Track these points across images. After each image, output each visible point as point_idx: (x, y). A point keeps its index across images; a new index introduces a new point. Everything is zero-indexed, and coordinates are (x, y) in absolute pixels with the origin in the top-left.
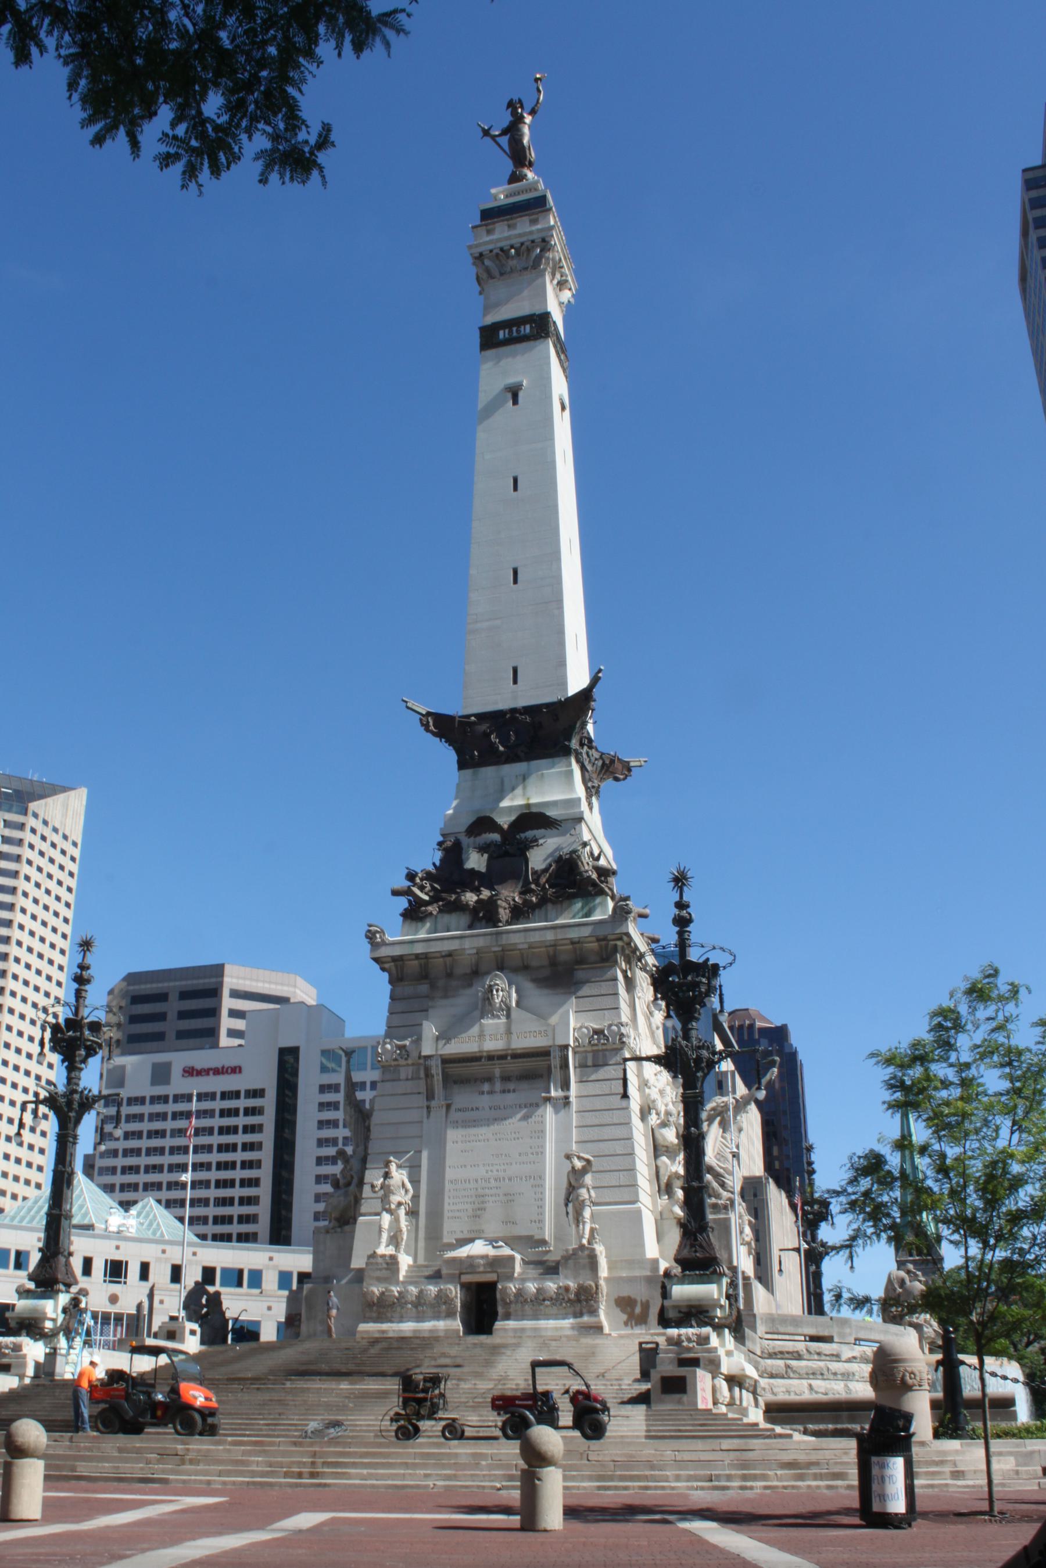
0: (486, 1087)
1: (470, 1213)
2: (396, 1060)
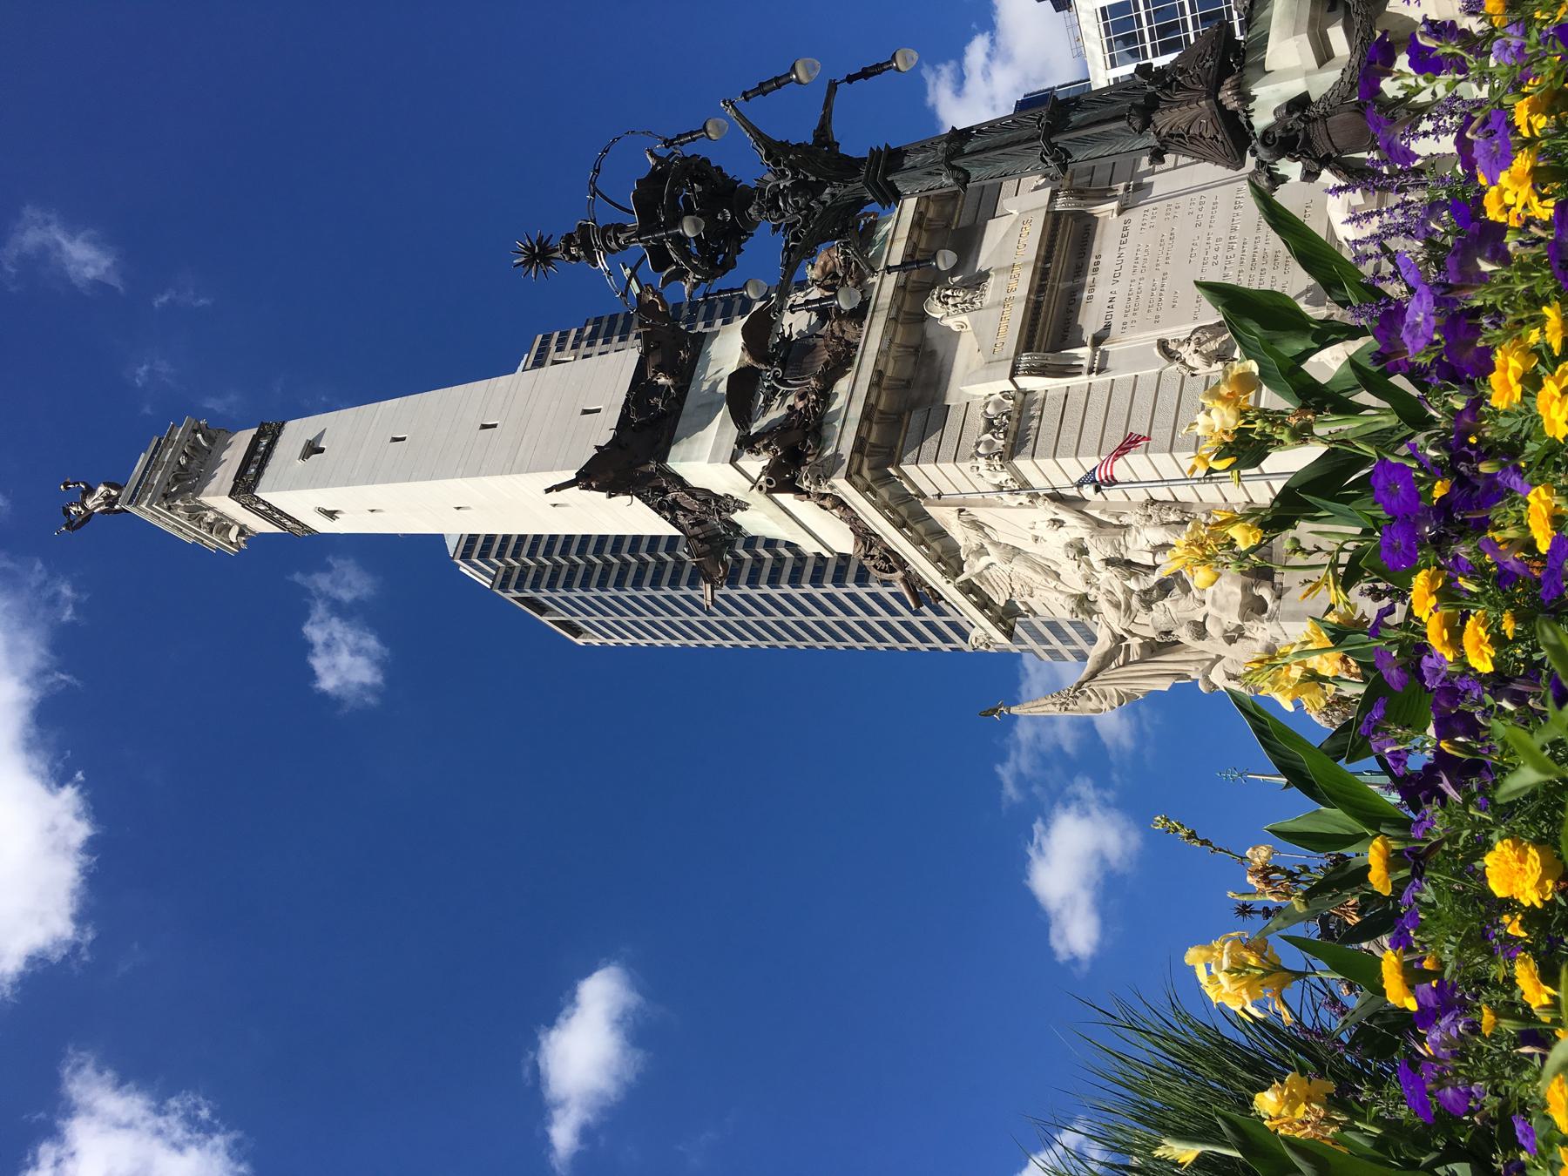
0: (1086, 294)
2: (1005, 433)
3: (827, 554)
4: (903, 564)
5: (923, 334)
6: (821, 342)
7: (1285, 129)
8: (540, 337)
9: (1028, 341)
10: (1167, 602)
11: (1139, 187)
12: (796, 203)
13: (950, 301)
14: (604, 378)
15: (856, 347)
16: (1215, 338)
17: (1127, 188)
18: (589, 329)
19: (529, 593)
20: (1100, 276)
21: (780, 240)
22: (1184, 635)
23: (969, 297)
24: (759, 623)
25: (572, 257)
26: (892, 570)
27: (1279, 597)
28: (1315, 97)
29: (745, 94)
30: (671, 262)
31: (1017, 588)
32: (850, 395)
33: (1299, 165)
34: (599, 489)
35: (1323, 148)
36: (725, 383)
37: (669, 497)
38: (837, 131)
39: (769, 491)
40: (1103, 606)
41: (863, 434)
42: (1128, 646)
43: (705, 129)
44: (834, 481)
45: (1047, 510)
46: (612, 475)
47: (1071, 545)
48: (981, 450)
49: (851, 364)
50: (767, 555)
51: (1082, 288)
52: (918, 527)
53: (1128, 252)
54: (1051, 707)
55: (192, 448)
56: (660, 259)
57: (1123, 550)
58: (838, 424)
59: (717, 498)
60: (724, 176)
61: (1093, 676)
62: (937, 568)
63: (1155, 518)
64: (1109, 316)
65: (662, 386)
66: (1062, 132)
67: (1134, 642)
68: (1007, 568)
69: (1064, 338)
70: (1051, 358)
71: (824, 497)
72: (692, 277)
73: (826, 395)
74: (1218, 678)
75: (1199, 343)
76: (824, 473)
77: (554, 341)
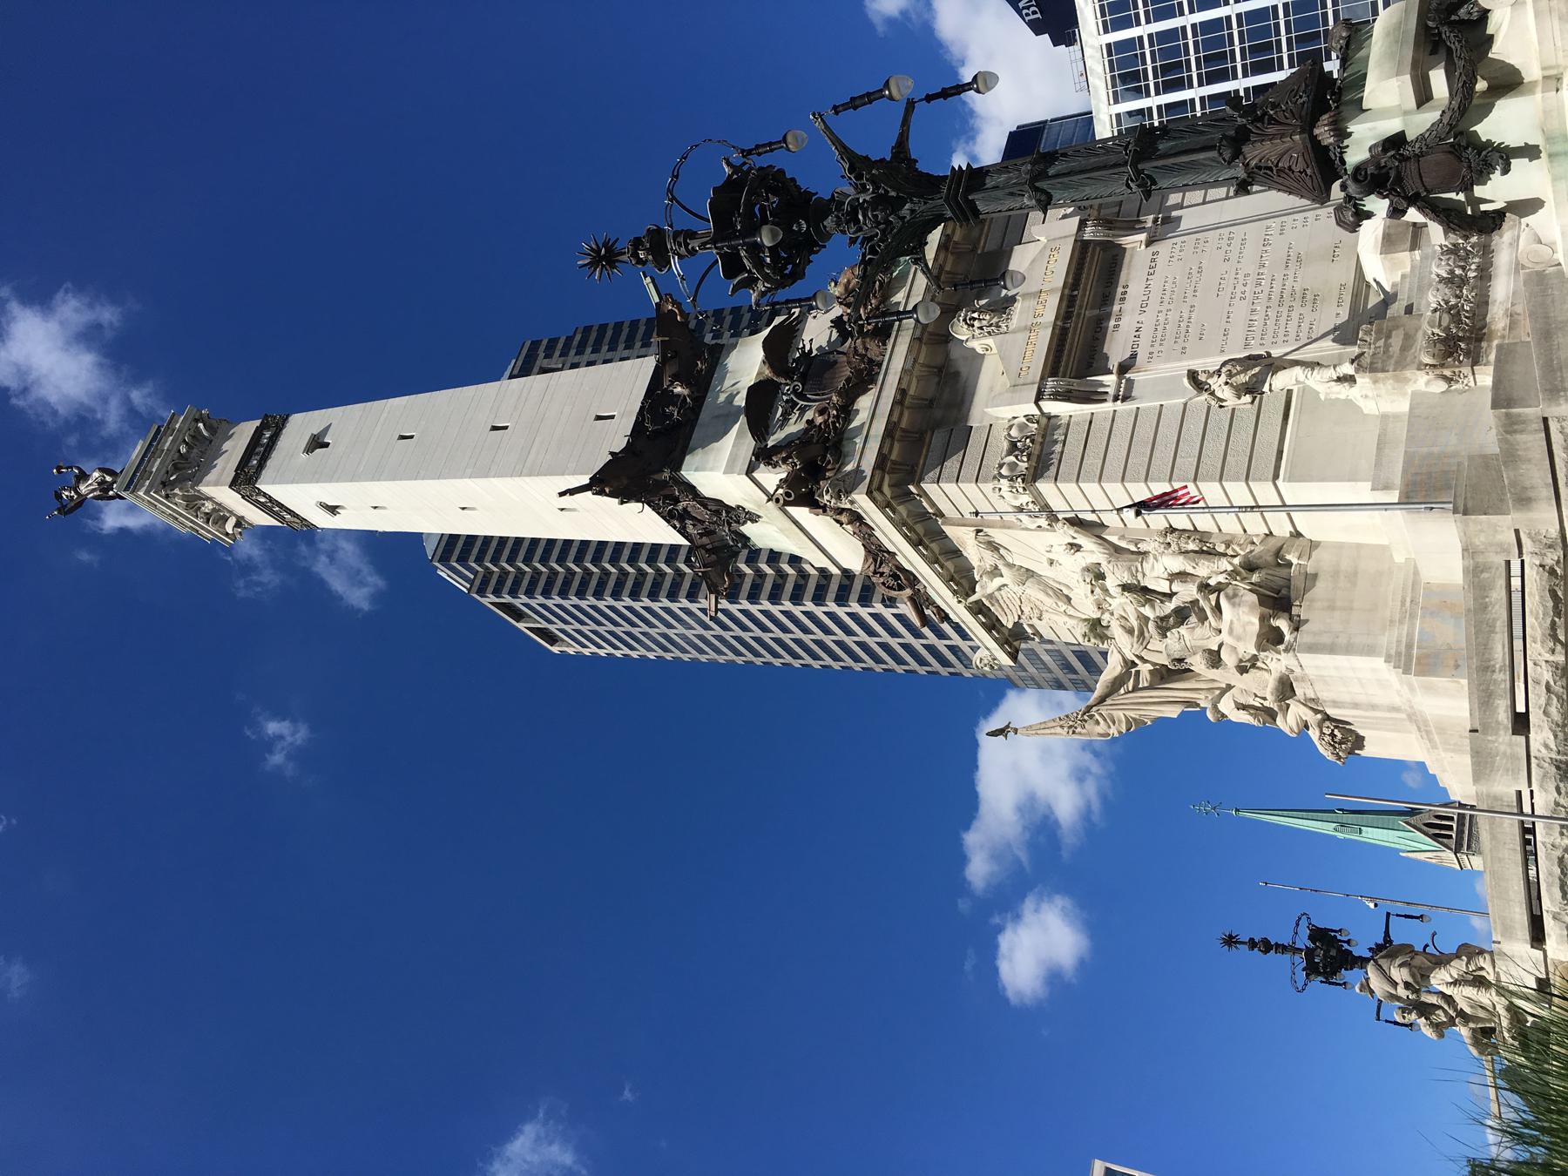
0: (1112, 323)
1: (1306, 311)
2: (1029, 456)
3: (834, 570)
4: (912, 580)
5: (947, 354)
6: (843, 359)
7: (1378, 167)
8: (528, 343)
9: (1054, 366)
10: (1183, 630)
11: (1168, 220)
12: (876, 216)
13: (976, 324)
14: (624, 384)
15: (880, 365)
16: (1244, 371)
17: (1155, 221)
18: (578, 337)
19: (507, 599)
20: (1127, 306)
21: (857, 252)
22: (1198, 663)
23: (995, 320)
24: (776, 640)
25: (639, 261)
26: (901, 588)
27: (1297, 629)
28: (1410, 136)
29: (835, 108)
30: (743, 269)
31: (1026, 610)
32: (872, 412)
33: (1386, 202)
34: (611, 495)
35: (1412, 186)
36: (744, 394)
37: (680, 506)
38: (915, 149)
39: (787, 503)
40: (1116, 631)
41: (885, 451)
42: (1138, 672)
43: (784, 140)
44: (854, 496)
45: (1065, 534)
46: (625, 481)
47: (1087, 569)
48: (1004, 471)
49: (873, 381)
50: (790, 571)
51: (1108, 316)
52: (934, 546)
53: (1156, 283)
54: (1059, 730)
55: (193, 437)
56: (732, 266)
57: (1140, 576)
58: (859, 441)
59: (729, 509)
60: (799, 188)
61: (1102, 700)
62: (949, 587)
63: (1174, 547)
64: (1135, 345)
65: (678, 395)
66: (1149, 159)
67: (1144, 669)
68: (1019, 590)
69: (1090, 365)
70: (1076, 384)
71: (841, 511)
72: (761, 287)
73: (847, 411)
74: (1226, 706)
75: (1230, 375)
76: (845, 487)
77: (542, 348)
